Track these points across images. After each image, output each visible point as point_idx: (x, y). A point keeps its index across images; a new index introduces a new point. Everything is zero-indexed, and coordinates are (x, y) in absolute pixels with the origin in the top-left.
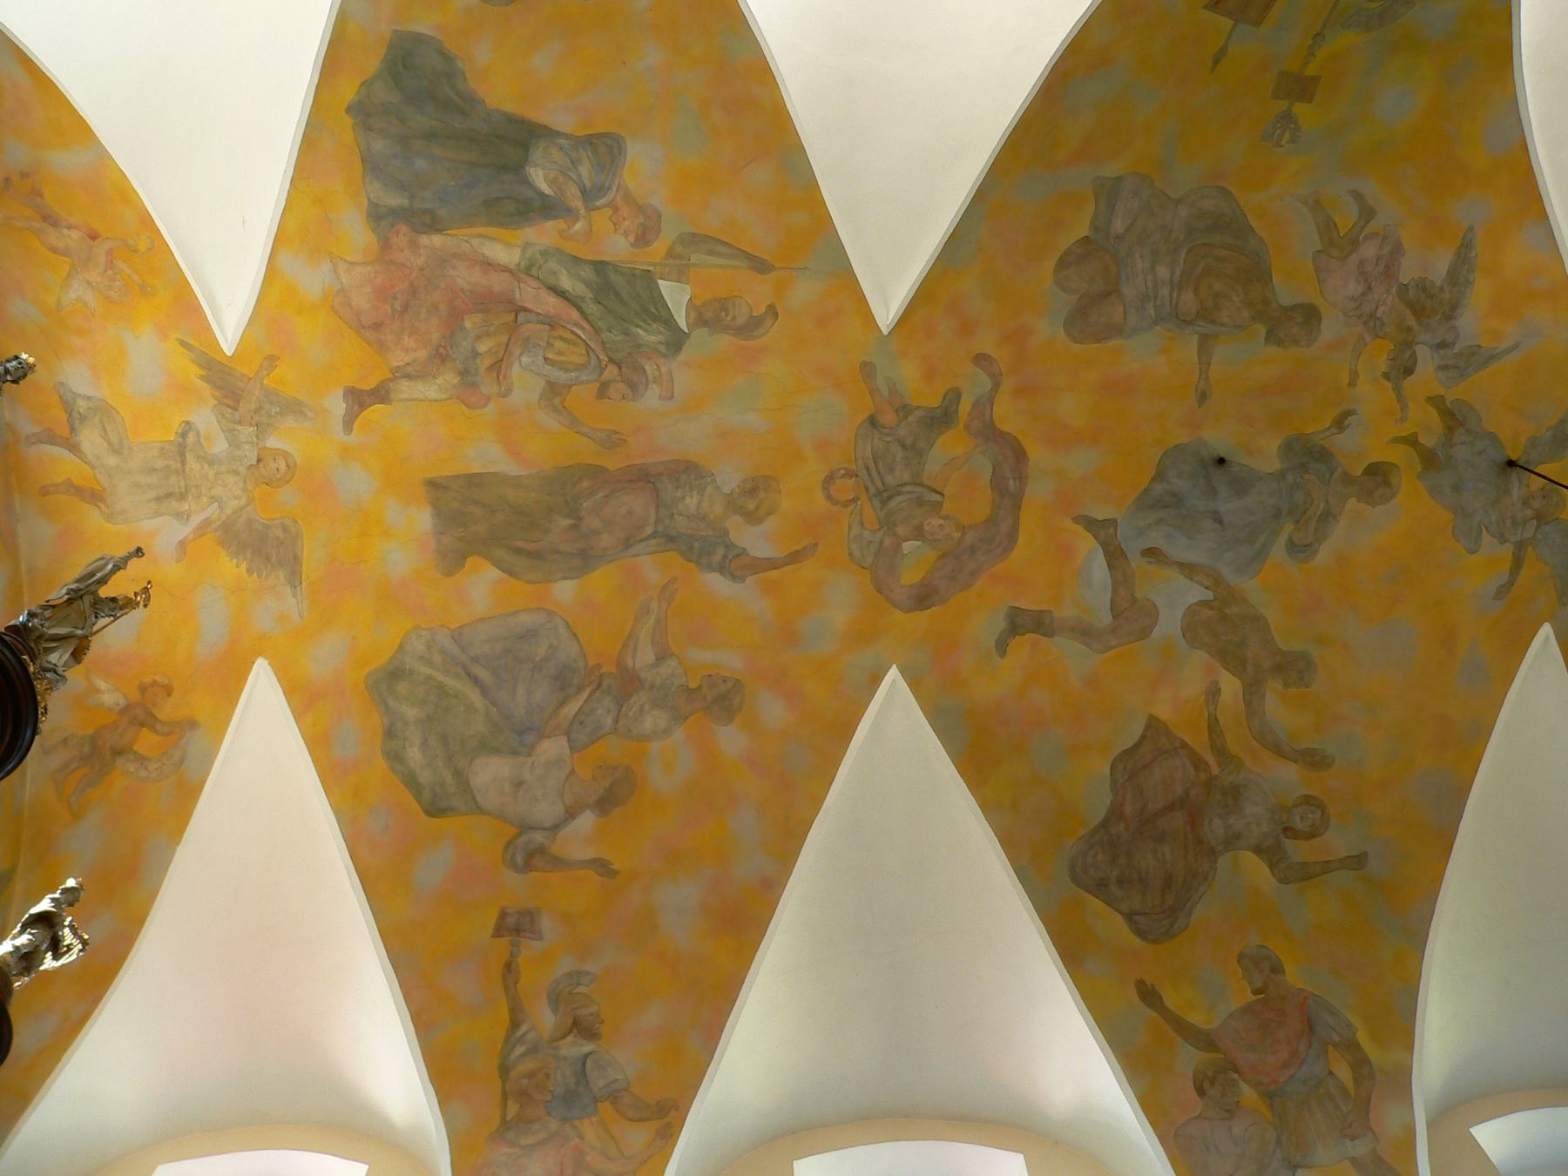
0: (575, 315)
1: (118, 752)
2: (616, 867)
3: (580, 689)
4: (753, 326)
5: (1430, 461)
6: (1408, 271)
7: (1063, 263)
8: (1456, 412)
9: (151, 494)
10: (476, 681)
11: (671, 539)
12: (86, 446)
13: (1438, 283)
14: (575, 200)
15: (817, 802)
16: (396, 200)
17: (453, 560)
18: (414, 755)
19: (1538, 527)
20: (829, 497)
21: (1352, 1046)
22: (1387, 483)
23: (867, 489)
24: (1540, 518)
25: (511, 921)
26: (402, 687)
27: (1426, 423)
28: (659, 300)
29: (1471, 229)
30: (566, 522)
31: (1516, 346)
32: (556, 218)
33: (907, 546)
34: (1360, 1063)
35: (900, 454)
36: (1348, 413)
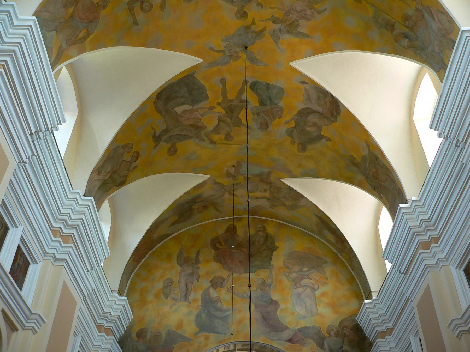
5: (247, 28)
6: (302, 22)
8: (261, 34)
13: (298, 30)
19: (229, 56)
21: (88, 34)
22: (241, 17)
24: (232, 55)
27: (259, 26)
29: (312, 38)
31: (279, 48)
34: (85, 38)
36: (262, 7)
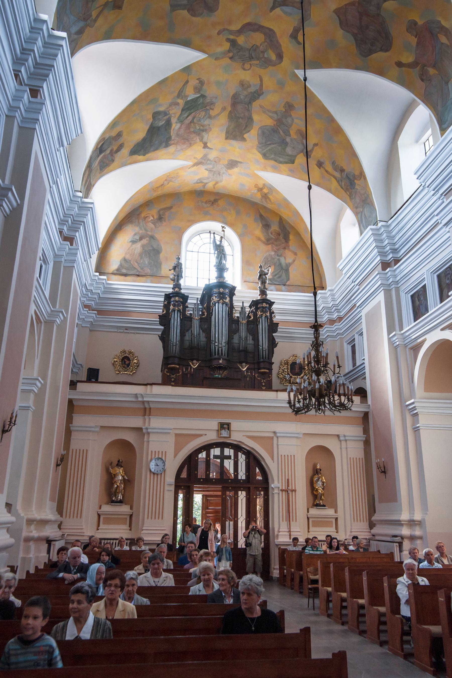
0: (193, 114)
1: (266, 195)
2: (316, 143)
3: (278, 129)
4: (202, 83)
7: (194, 15)
9: (218, 175)
10: (270, 144)
11: (250, 103)
12: (207, 182)
14: (166, 118)
15: (320, 101)
16: (164, 144)
17: (244, 140)
18: (281, 159)
20: (248, 70)
23: (248, 61)
25: (318, 165)
26: (267, 155)
28: (192, 100)
30: (241, 120)
32: (171, 119)
33: (266, 56)
35: (241, 53)
